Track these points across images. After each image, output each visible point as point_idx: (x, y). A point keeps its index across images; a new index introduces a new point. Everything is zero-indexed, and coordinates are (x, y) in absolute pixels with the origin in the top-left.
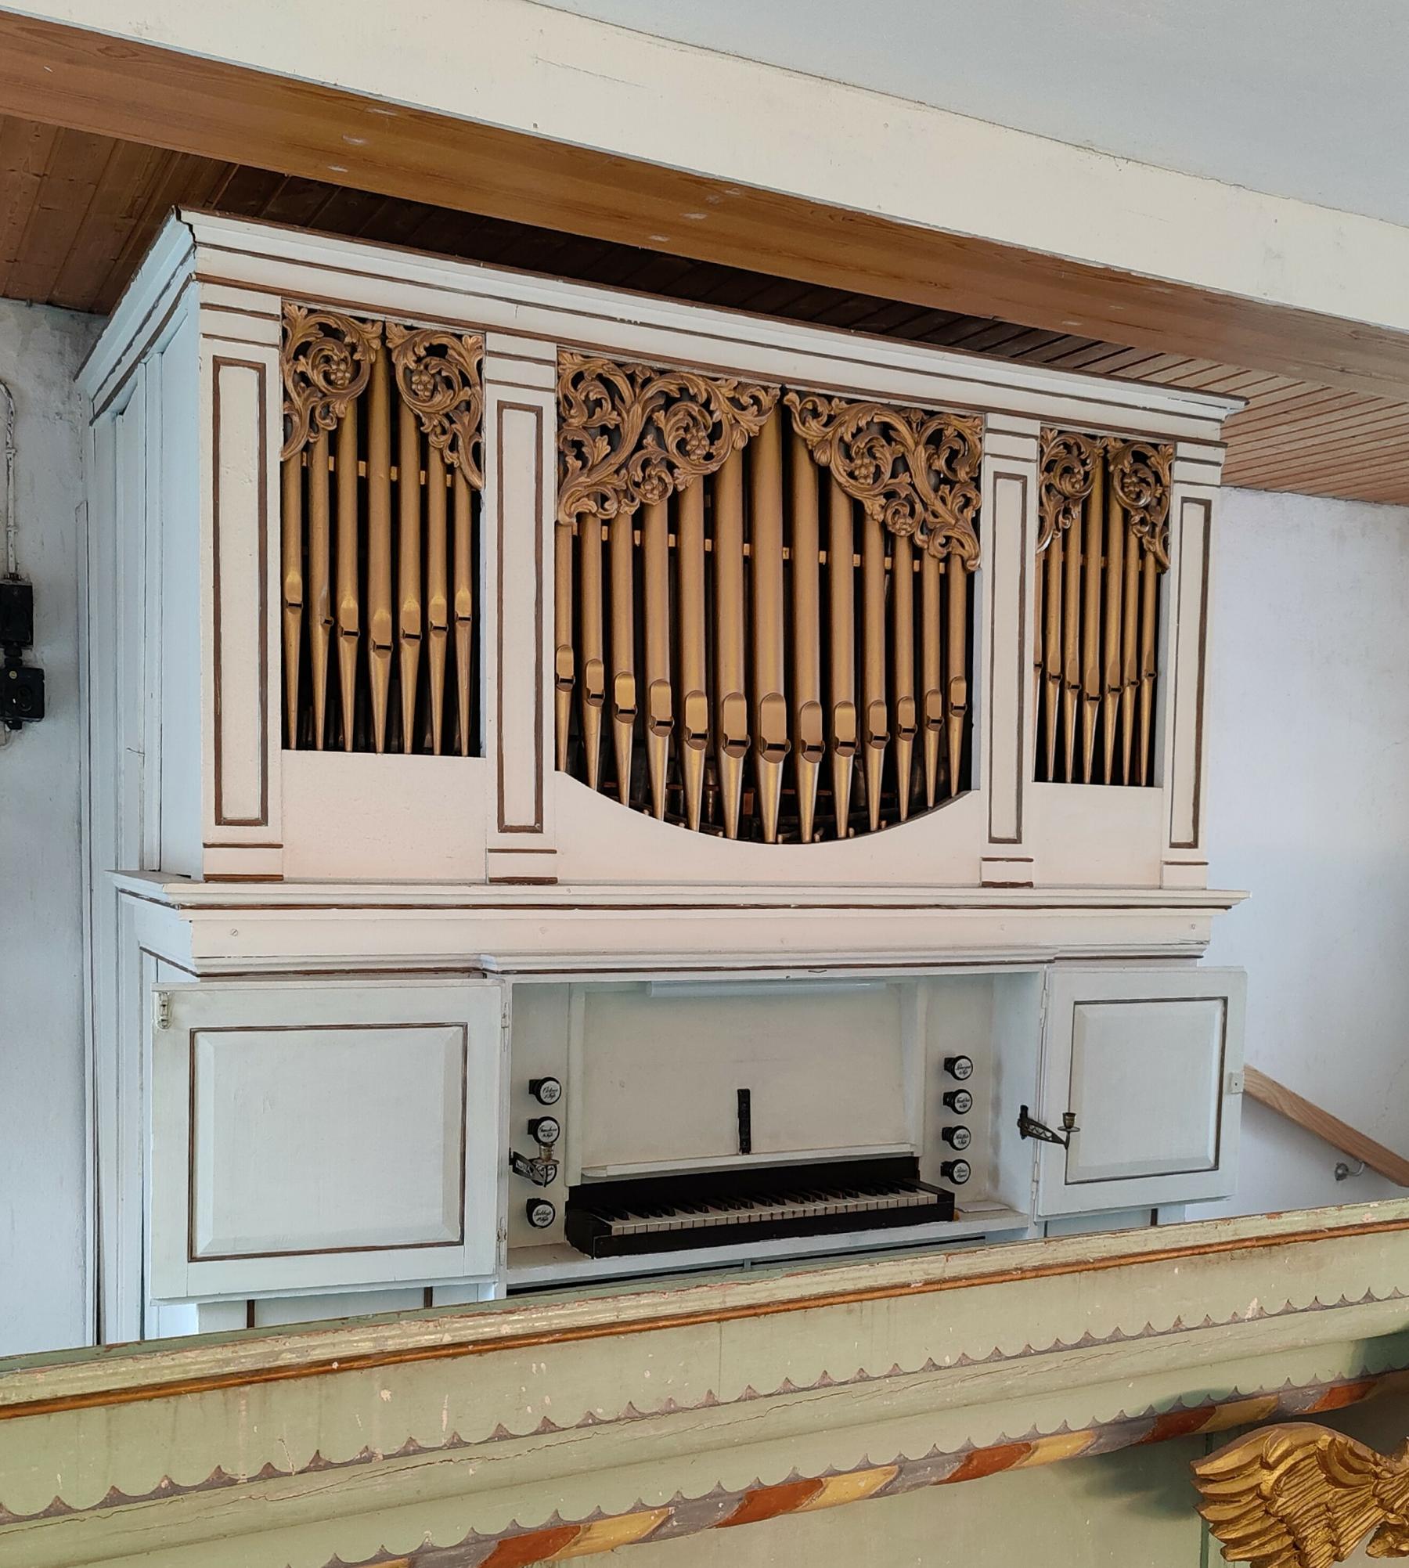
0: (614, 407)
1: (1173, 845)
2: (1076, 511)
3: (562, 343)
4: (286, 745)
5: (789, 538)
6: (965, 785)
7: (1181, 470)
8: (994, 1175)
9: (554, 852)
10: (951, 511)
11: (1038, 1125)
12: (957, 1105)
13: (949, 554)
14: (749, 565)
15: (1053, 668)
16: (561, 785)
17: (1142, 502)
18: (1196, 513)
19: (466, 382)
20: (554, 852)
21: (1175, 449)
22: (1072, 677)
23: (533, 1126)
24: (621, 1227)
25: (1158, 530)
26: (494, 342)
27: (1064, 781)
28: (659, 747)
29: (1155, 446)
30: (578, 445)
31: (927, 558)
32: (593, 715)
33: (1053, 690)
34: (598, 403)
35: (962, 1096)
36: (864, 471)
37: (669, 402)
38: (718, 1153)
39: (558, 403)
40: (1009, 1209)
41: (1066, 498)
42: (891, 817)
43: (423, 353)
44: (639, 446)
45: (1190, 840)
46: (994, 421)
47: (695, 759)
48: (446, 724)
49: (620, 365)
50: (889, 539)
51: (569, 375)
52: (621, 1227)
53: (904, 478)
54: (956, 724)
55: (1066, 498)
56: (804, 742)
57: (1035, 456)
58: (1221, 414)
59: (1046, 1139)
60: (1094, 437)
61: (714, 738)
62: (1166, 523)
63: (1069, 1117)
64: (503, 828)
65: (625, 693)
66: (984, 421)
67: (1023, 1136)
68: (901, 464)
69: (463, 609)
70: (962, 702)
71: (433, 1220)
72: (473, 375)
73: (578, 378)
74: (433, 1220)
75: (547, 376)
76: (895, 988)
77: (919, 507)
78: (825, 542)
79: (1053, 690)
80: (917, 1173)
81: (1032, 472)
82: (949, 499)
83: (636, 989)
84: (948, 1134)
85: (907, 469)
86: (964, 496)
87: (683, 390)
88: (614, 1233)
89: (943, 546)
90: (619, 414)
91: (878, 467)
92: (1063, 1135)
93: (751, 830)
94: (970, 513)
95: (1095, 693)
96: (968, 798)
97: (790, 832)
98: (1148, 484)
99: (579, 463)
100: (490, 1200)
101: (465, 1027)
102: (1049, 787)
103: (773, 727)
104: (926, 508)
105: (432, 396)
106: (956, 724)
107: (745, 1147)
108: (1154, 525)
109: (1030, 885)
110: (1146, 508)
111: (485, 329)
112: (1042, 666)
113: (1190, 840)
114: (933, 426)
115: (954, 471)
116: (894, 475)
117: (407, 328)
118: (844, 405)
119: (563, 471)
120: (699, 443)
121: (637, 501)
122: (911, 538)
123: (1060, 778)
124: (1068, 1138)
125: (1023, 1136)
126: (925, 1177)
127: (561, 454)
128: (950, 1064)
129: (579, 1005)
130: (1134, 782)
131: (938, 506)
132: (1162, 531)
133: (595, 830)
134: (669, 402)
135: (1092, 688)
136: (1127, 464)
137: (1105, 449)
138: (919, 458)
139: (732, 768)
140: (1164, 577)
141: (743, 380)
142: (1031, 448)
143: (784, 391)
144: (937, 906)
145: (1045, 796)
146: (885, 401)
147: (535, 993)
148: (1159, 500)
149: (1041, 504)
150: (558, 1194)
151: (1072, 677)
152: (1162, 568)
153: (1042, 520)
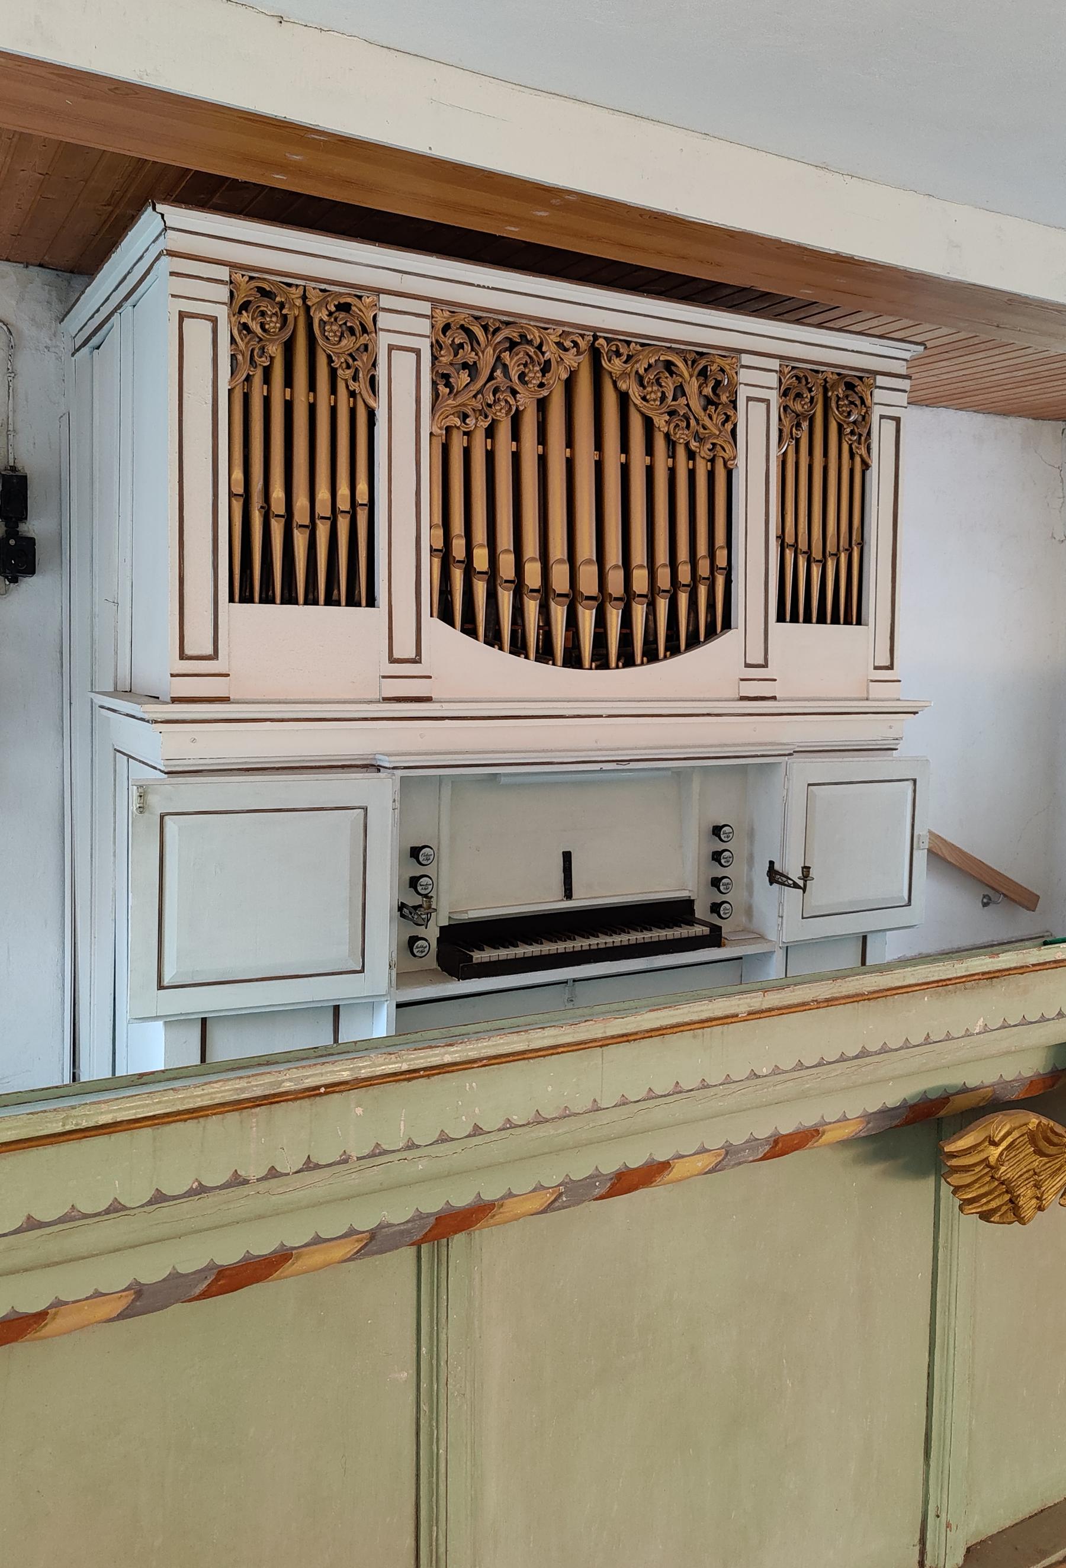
0: (473, 349)
1: (876, 668)
2: (805, 425)
3: (435, 302)
4: (231, 600)
5: (599, 445)
6: (727, 625)
7: (879, 395)
8: (749, 911)
9: (430, 677)
10: (716, 425)
11: (782, 875)
12: (723, 861)
13: (715, 456)
14: (570, 465)
15: (789, 539)
16: (434, 626)
17: (852, 419)
18: (889, 426)
19: (365, 330)
20: (430, 677)
21: (875, 380)
22: (803, 546)
23: (414, 882)
24: (479, 956)
25: (863, 438)
26: (385, 301)
27: (797, 621)
28: (506, 599)
29: (861, 378)
30: (446, 377)
31: (698, 459)
32: (458, 576)
33: (789, 555)
34: (461, 346)
35: (726, 854)
36: (653, 396)
37: (512, 345)
38: (548, 899)
39: (432, 346)
40: (761, 937)
41: (798, 415)
42: (673, 649)
43: (333, 309)
44: (491, 377)
45: (888, 664)
46: (746, 359)
47: (532, 607)
48: (350, 584)
49: (477, 318)
50: (671, 444)
51: (440, 325)
52: (479, 956)
53: (682, 401)
54: (720, 580)
55: (798, 415)
56: (610, 595)
57: (775, 384)
58: (907, 355)
59: (789, 886)
60: (817, 372)
61: (545, 592)
62: (869, 434)
63: (806, 870)
64: (392, 660)
65: (481, 559)
66: (739, 360)
67: (771, 884)
68: (680, 391)
69: (362, 497)
70: (724, 564)
71: (342, 955)
72: (370, 326)
73: (446, 328)
74: (342, 955)
75: (424, 326)
76: (674, 775)
77: (693, 422)
78: (625, 448)
79: (789, 555)
80: (692, 912)
81: (773, 396)
82: (714, 417)
83: (489, 778)
84: (716, 882)
85: (684, 394)
86: (725, 414)
87: (523, 336)
88: (474, 961)
89: (710, 450)
90: (477, 354)
91: (663, 393)
92: (801, 883)
93: (572, 660)
94: (729, 426)
95: (819, 557)
96: (730, 634)
97: (601, 661)
98: (856, 405)
99: (448, 390)
100: (383, 937)
101: (365, 809)
102: (788, 627)
103: (588, 584)
104: (698, 424)
105: (340, 340)
106: (720, 580)
107: (568, 894)
108: (860, 435)
109: (774, 698)
110: (854, 422)
111: (379, 291)
112: (781, 538)
113: (888, 664)
114: (703, 363)
115: (718, 396)
116: (675, 399)
117: (322, 291)
118: (639, 348)
119: (436, 396)
120: (534, 375)
121: (490, 418)
122: (687, 445)
123: (794, 619)
124: (805, 885)
125: (771, 884)
126: (698, 915)
127: (434, 383)
128: (717, 831)
129: (446, 792)
130: (848, 622)
131: (707, 422)
132: (866, 440)
133: (459, 659)
134: (512, 345)
135: (817, 554)
136: (841, 391)
137: (825, 380)
138: (692, 386)
139: (559, 614)
140: (868, 472)
141: (566, 329)
142: (772, 380)
143: (596, 338)
144: (709, 715)
145: (785, 633)
146: (668, 345)
147: (418, 782)
148: (864, 417)
149: (780, 419)
150: (432, 933)
152: (866, 466)
153: (781, 431)
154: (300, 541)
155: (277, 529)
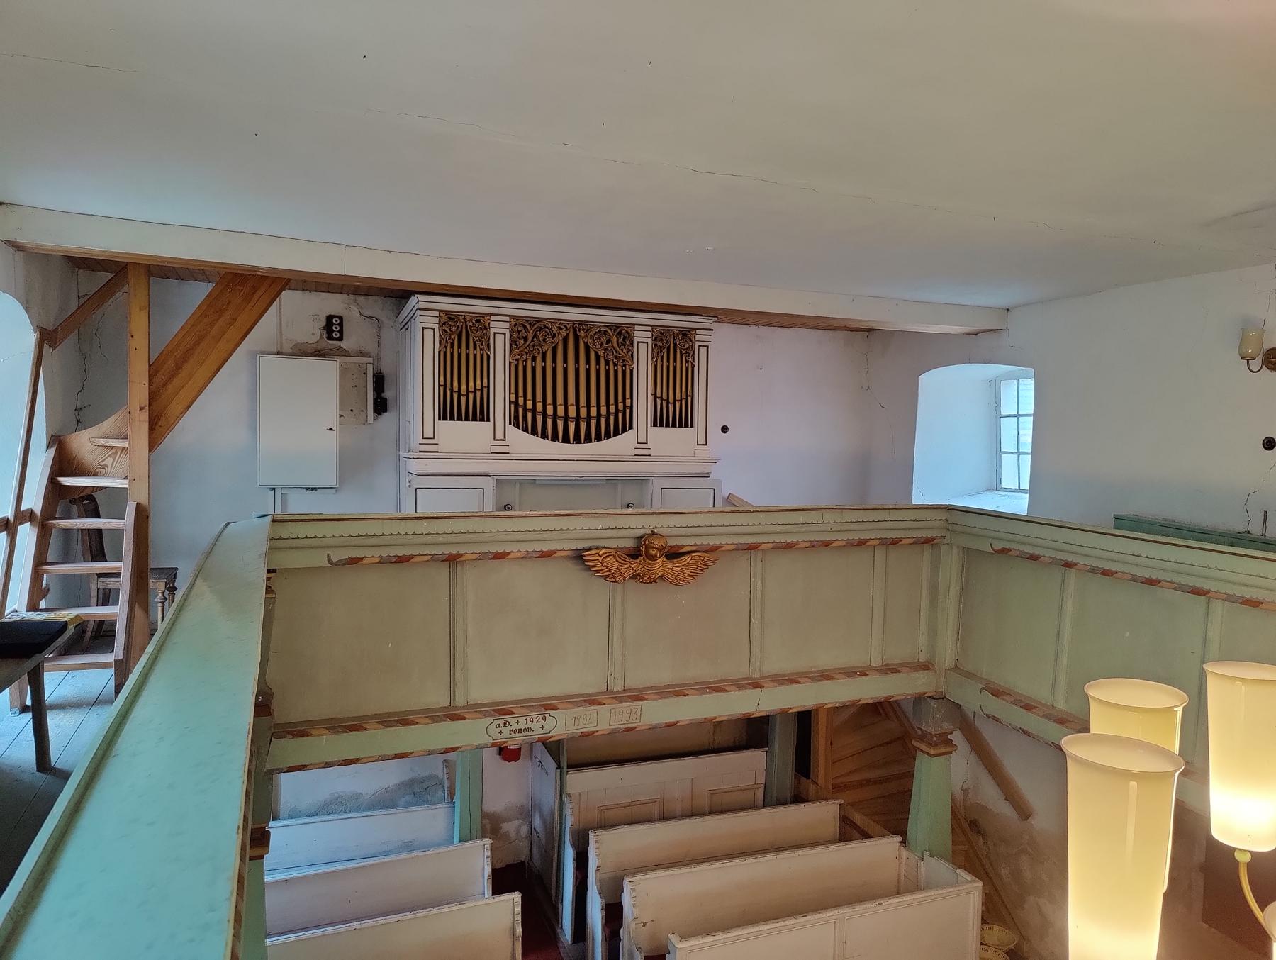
5: (577, 361)
22: (665, 397)
28: (539, 419)
48: (480, 413)
81: (649, 341)
135: (671, 400)
139: (560, 424)
142: (649, 334)
145: (656, 432)
151: (665, 397)
154: (463, 400)
155: (455, 396)
